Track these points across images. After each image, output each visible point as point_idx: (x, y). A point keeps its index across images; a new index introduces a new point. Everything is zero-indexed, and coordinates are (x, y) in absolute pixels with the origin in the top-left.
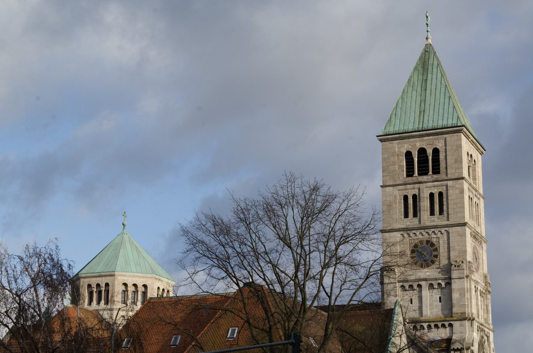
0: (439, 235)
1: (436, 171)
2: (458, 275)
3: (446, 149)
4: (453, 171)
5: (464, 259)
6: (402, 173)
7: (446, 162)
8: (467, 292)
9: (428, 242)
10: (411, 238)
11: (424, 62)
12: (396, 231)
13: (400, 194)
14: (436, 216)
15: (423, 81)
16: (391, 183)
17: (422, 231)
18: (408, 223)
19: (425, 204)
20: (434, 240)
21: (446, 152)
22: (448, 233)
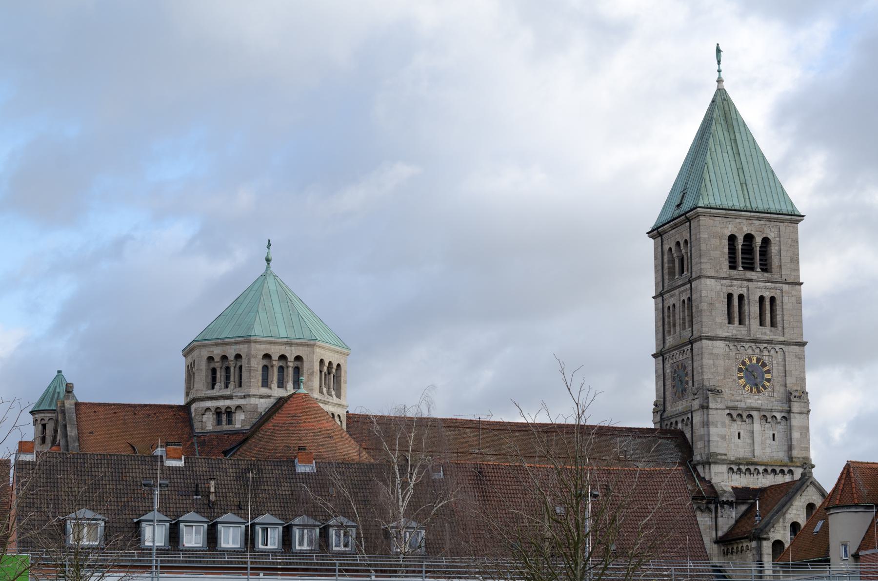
0: (773, 352)
1: (766, 268)
4: (789, 273)
12: (721, 340)
13: (724, 291)
15: (732, 141)
16: (713, 274)
17: (753, 345)
19: (753, 309)
20: (766, 359)
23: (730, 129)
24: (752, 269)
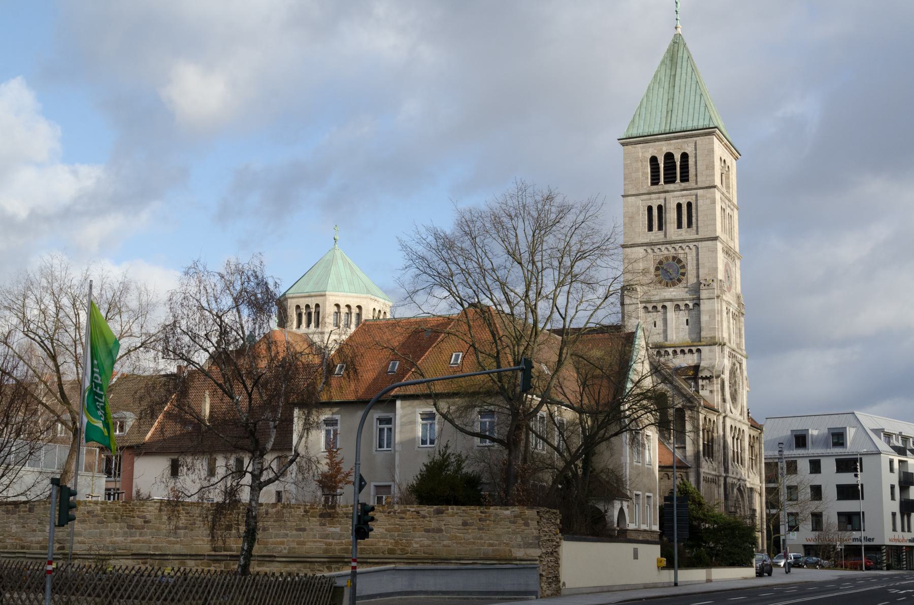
0: (687, 250)
1: (685, 178)
2: (708, 295)
3: (696, 154)
4: (704, 179)
5: (715, 277)
6: (646, 181)
7: (696, 169)
8: (718, 314)
9: (674, 258)
10: (655, 254)
11: (673, 54)
12: (639, 246)
14: (683, 229)
16: (634, 193)
17: (668, 246)
18: (653, 237)
19: (671, 216)
20: (681, 257)
21: (696, 157)
22: (697, 248)
23: (673, 67)
24: (673, 182)
